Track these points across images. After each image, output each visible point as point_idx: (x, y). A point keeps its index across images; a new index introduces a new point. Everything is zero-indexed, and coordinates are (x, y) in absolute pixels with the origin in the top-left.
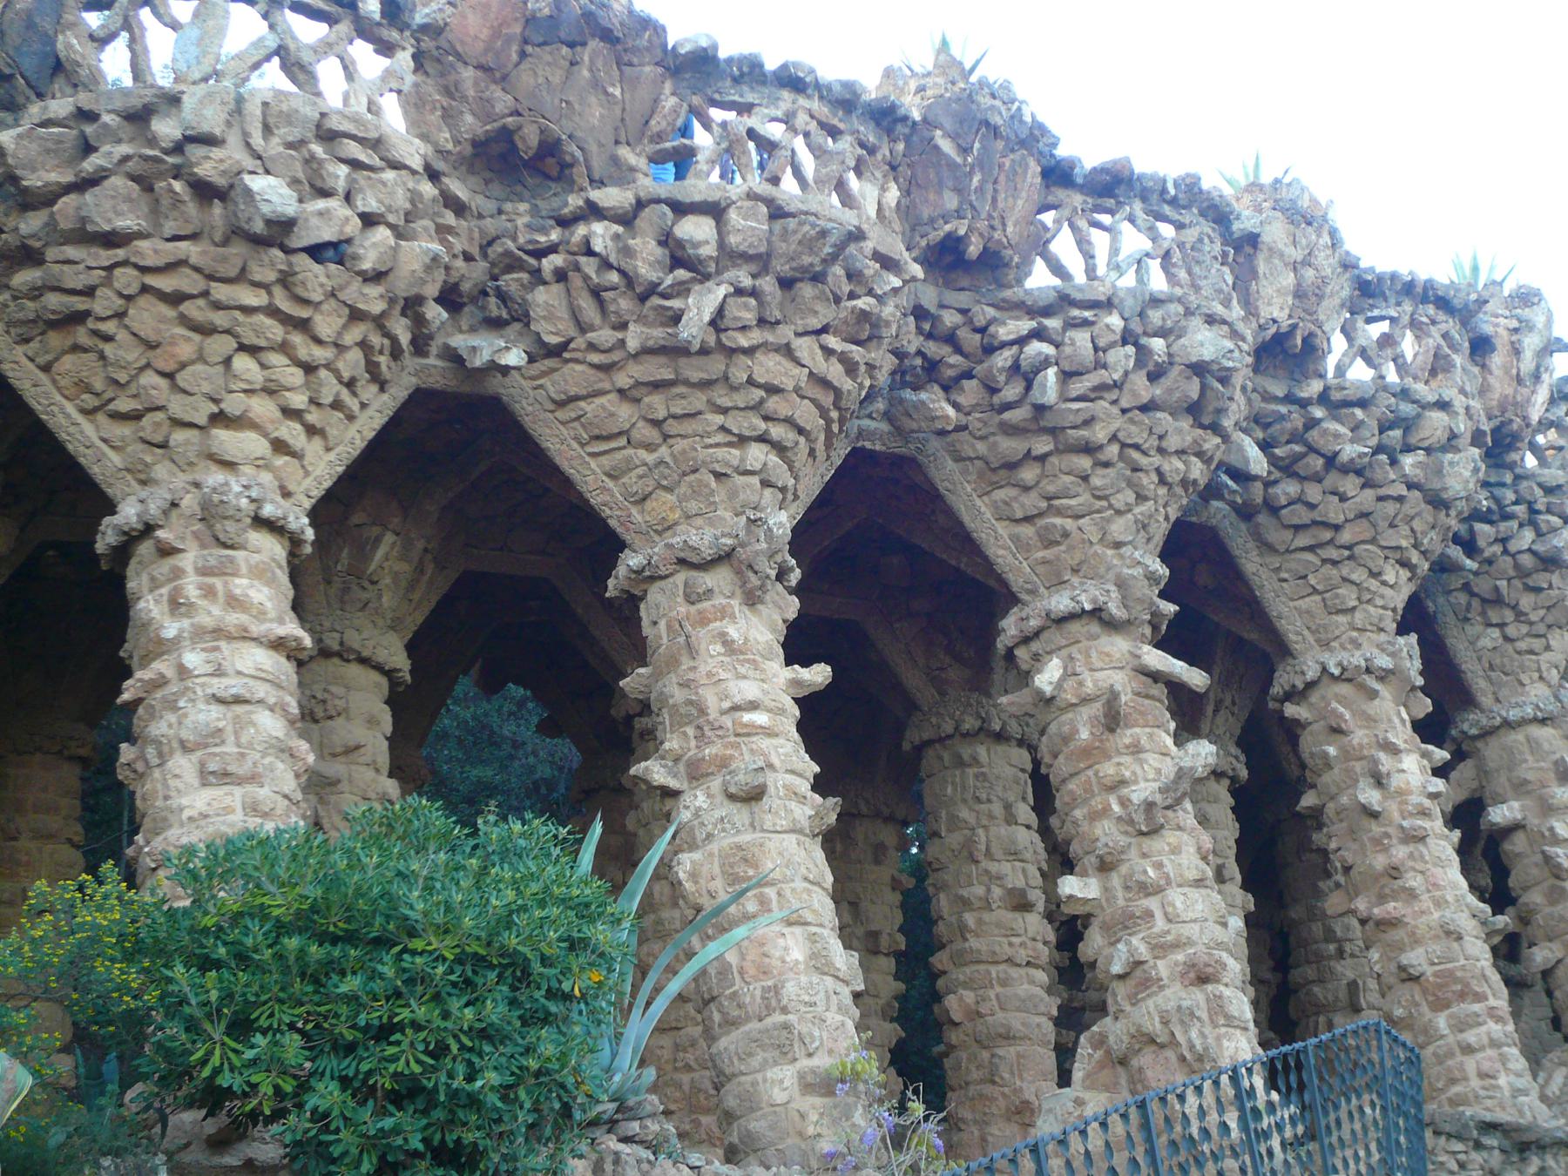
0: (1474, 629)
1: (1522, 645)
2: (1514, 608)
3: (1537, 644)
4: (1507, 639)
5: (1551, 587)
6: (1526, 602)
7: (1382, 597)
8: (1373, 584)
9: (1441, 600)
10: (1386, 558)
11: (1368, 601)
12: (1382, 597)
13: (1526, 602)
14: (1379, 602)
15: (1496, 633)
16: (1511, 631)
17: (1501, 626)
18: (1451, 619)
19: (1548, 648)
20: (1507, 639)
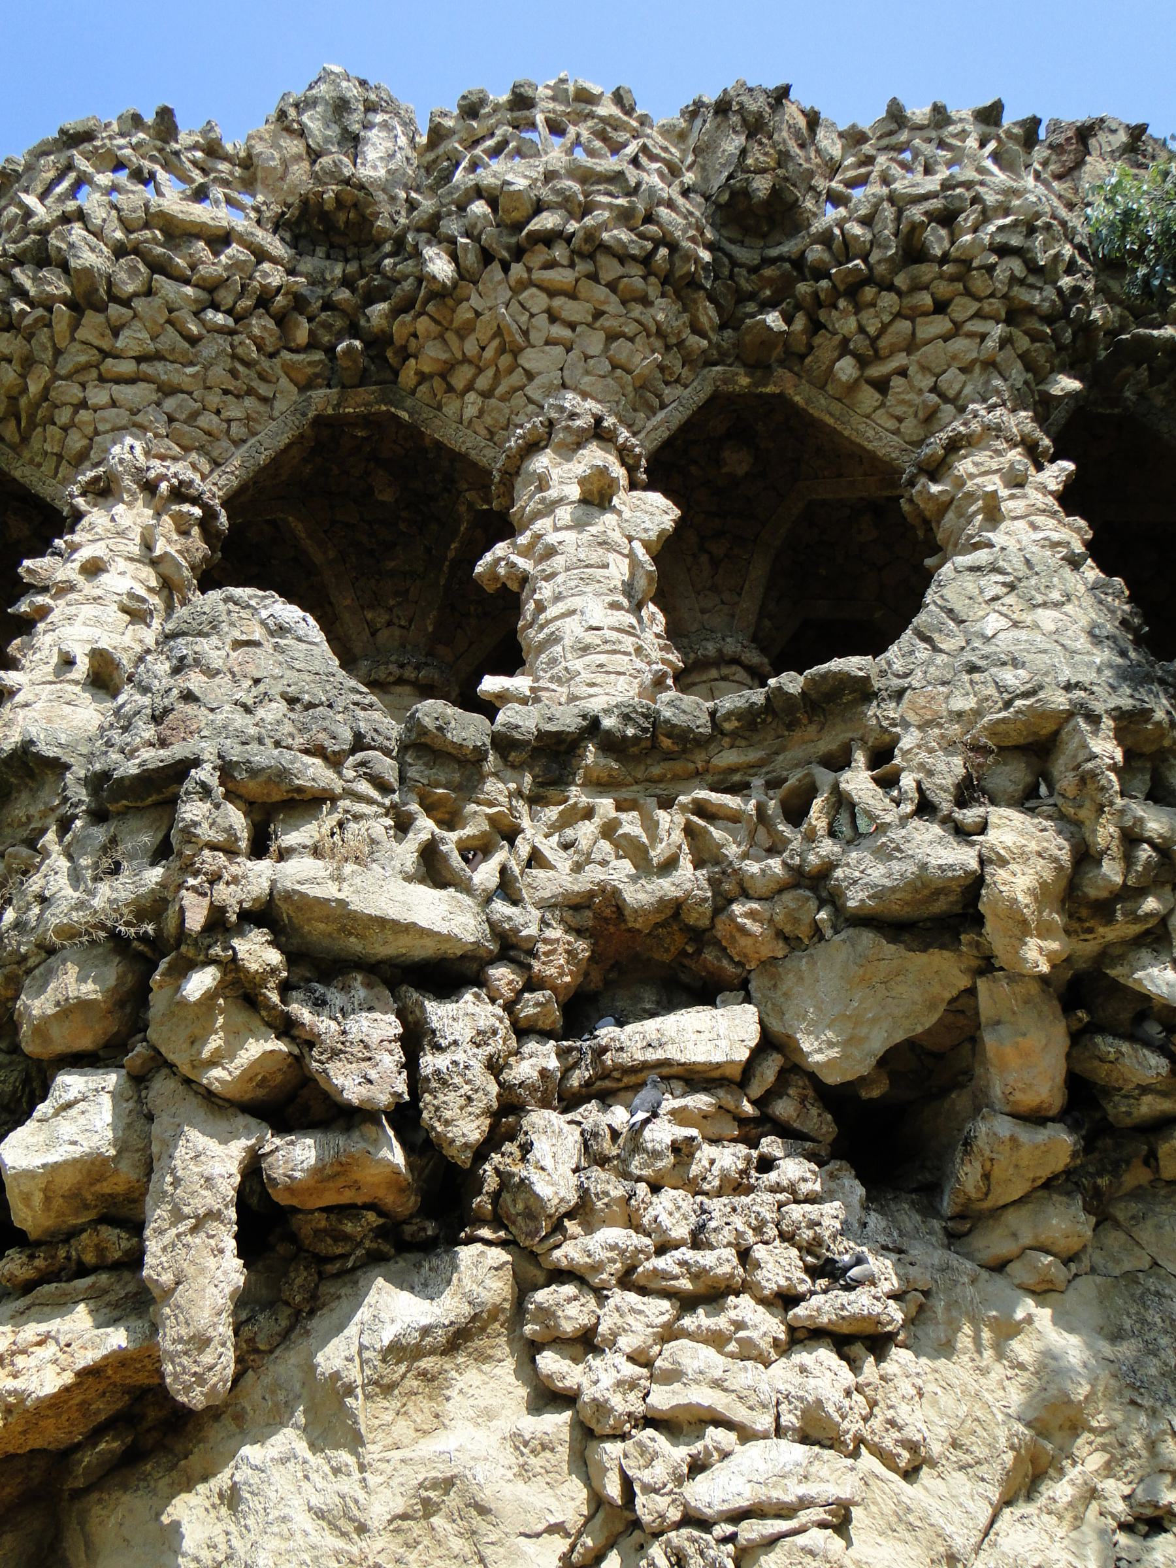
0: (451, 408)
1: (500, 390)
2: (466, 360)
3: (517, 378)
4: (486, 395)
5: (478, 314)
6: (471, 347)
7: (104, 420)
8: (84, 415)
9: (409, 402)
10: (83, 386)
11: (97, 433)
12: (104, 420)
13: (471, 347)
14: (108, 426)
15: (471, 397)
16: (483, 382)
17: (470, 387)
18: (427, 413)
19: (530, 376)
20: (486, 395)
